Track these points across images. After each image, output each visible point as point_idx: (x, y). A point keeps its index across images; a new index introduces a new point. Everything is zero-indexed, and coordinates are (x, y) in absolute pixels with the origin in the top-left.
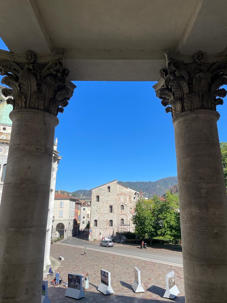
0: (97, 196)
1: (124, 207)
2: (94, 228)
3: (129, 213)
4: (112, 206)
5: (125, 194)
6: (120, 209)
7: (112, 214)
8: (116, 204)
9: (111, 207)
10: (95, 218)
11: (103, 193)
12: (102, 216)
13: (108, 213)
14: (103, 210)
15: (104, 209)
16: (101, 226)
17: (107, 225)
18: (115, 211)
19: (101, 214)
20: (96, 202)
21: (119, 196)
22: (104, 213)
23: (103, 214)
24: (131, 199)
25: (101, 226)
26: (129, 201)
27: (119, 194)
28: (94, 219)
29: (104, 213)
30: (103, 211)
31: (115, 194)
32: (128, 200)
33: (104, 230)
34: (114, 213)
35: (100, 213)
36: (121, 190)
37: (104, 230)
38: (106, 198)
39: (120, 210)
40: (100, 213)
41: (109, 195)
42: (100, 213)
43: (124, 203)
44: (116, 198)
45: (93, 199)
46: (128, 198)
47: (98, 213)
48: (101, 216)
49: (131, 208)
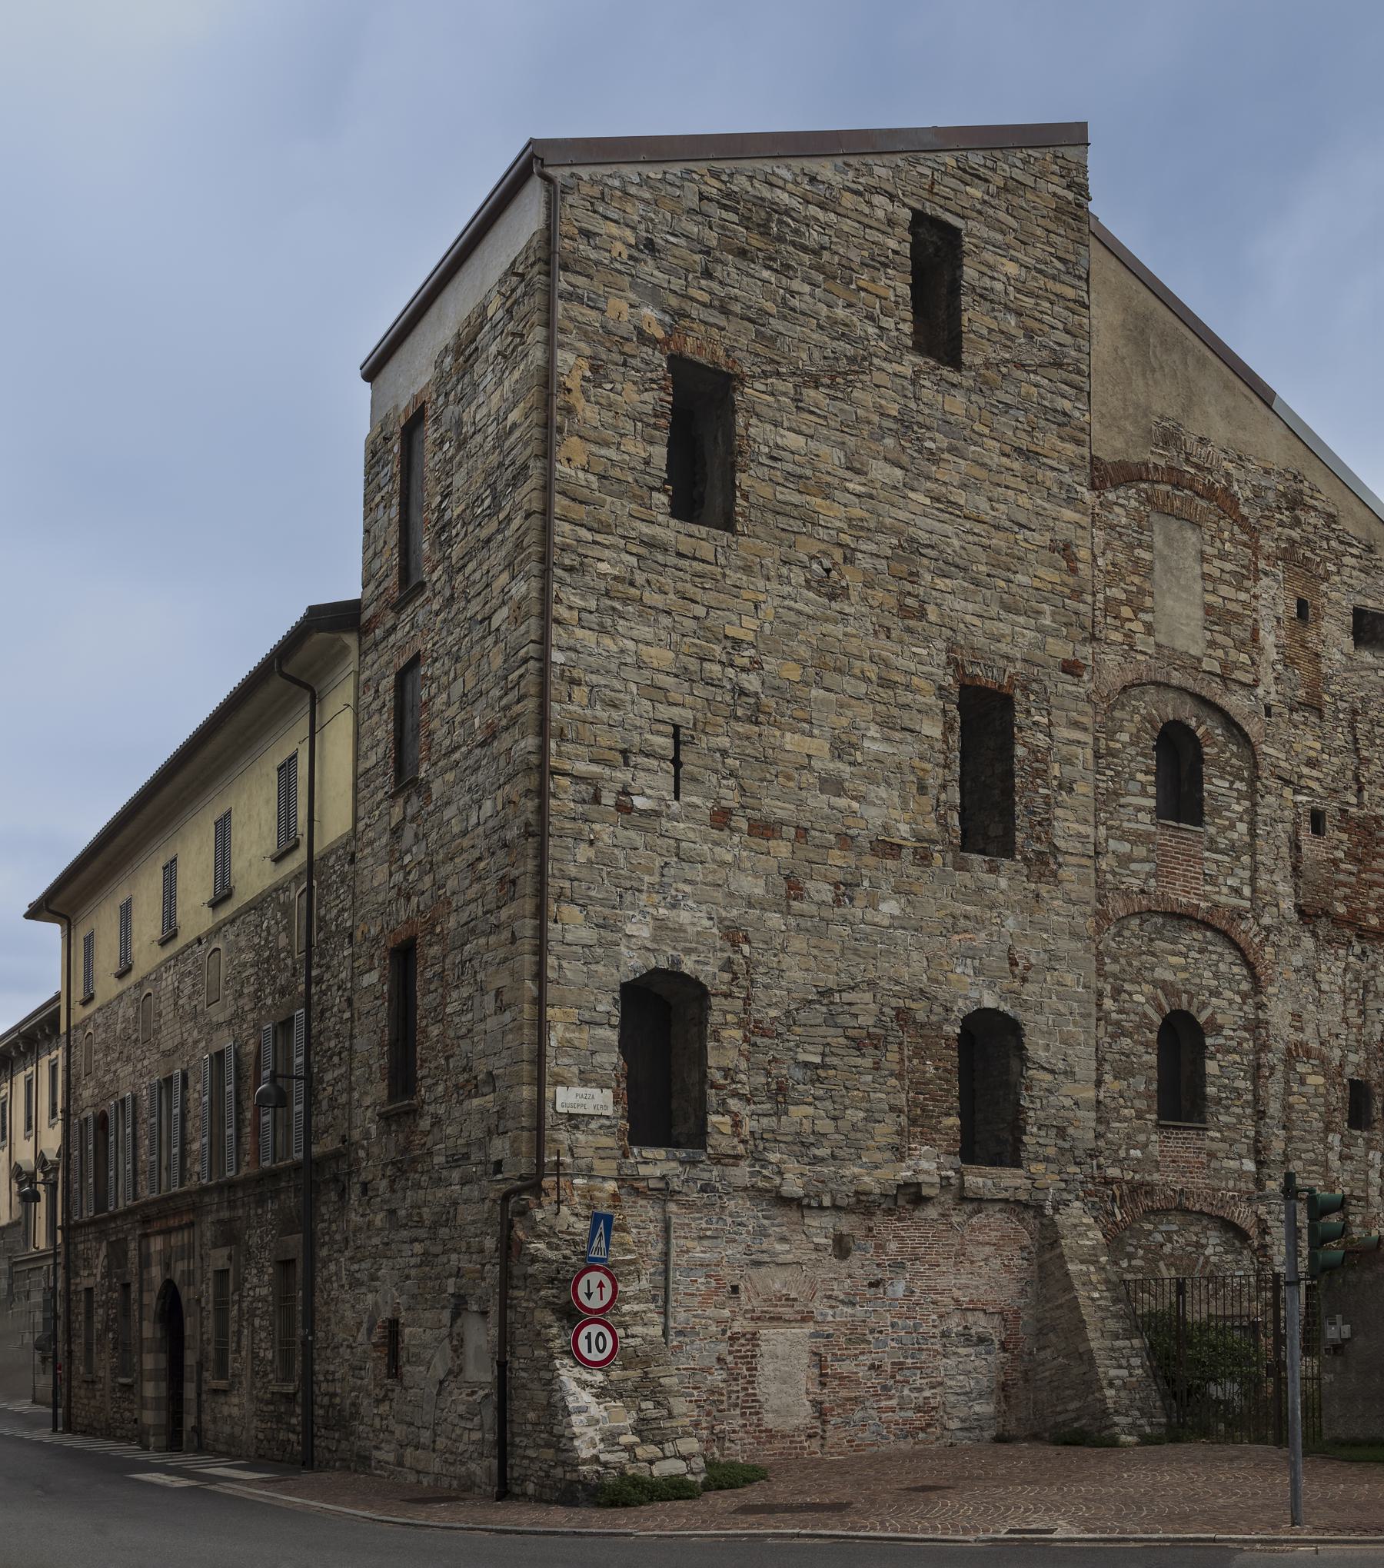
0: (678, 363)
1: (1216, 785)
2: (631, 1185)
3: (1287, 905)
4: (1005, 702)
5: (1225, 502)
6: (1141, 800)
7: (1005, 881)
8: (1071, 668)
9: (985, 717)
10: (643, 931)
11: (806, 346)
12: (820, 890)
13: (923, 858)
14: (818, 746)
15: (841, 749)
16: (802, 1145)
17: (917, 1123)
18: (1070, 826)
19: (782, 849)
20: (670, 531)
21: (1125, 502)
22: (845, 840)
23: (836, 857)
24: (1311, 636)
25: (802, 1145)
26: (1289, 662)
27: (1126, 475)
28: (633, 962)
29: (845, 840)
30: (833, 785)
31: (1049, 440)
32: (1268, 639)
33: (842, 1247)
34: (1044, 864)
35: (781, 810)
36: (1164, 402)
37: (842, 1247)
38: (881, 472)
39: (1145, 822)
40: (765, 829)
41: (947, 424)
42: (765, 829)
43: (1213, 690)
44: (1066, 550)
45: (588, 412)
46: (1272, 597)
47: (721, 818)
48: (794, 888)
49: (1317, 821)
